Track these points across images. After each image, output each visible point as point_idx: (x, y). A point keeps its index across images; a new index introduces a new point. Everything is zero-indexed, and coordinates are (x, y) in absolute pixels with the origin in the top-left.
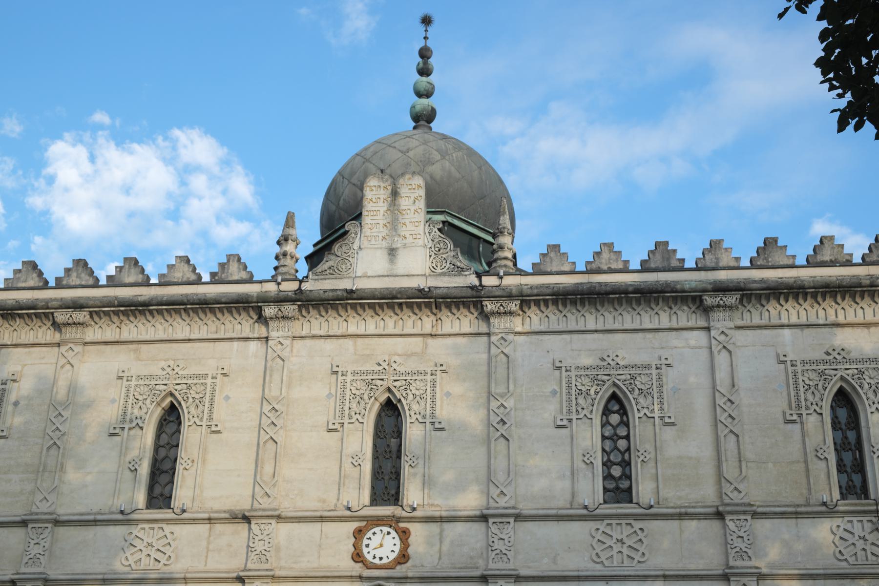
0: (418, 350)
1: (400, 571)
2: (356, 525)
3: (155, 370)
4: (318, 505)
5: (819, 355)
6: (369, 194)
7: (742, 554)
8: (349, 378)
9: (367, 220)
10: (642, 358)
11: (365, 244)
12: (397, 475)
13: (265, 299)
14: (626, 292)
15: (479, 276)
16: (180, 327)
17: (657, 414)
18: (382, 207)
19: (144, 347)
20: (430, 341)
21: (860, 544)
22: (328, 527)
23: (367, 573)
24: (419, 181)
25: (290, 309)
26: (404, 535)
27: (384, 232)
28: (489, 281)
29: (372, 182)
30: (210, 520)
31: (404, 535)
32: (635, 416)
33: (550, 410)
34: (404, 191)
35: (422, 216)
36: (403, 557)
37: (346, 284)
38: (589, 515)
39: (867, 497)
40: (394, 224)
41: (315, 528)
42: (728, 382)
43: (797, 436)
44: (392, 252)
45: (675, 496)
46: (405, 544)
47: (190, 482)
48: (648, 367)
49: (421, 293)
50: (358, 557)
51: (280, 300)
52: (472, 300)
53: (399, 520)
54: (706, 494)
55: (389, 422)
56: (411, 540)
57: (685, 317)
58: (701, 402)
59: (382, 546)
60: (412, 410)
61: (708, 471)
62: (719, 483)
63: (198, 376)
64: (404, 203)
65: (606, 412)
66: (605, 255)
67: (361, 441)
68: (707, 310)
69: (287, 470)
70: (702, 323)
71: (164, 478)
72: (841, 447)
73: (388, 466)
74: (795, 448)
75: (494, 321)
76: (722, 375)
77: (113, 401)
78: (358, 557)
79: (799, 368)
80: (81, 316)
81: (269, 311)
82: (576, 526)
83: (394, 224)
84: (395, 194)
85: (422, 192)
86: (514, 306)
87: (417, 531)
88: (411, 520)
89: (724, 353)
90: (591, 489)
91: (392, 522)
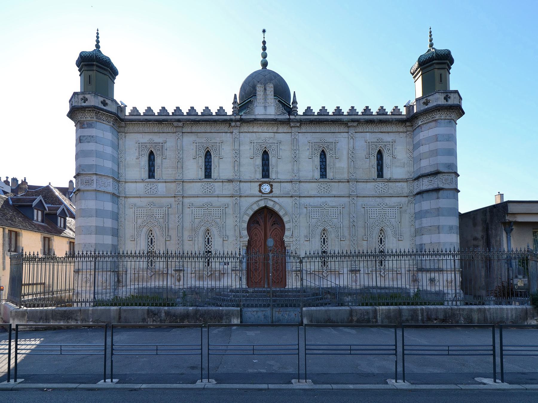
2: (259, 183)
3: (203, 140)
4: (249, 178)
5: (375, 140)
6: (258, 89)
7: (353, 191)
8: (255, 144)
9: (258, 97)
10: (331, 140)
11: (258, 105)
12: (268, 170)
13: (231, 120)
16: (208, 128)
17: (334, 156)
18: (262, 93)
19: (199, 134)
20: (276, 134)
21: (381, 189)
23: (263, 195)
24: (272, 86)
25: (238, 123)
27: (263, 101)
28: (292, 117)
29: (259, 85)
31: (271, 186)
32: (328, 156)
34: (268, 88)
35: (273, 97)
36: (271, 191)
37: (253, 117)
38: (316, 181)
39: (382, 177)
40: (265, 99)
41: (249, 184)
42: (352, 147)
43: (368, 162)
44: (265, 107)
45: (338, 177)
46: (272, 188)
47: (216, 171)
48: (332, 143)
49: (275, 120)
50: (260, 191)
51: (236, 121)
52: (287, 122)
53: (270, 182)
54: (345, 176)
55: (265, 156)
57: (342, 129)
58: (345, 153)
59: (266, 188)
61: (346, 170)
62: (348, 173)
63: (215, 143)
64: (268, 92)
65: (321, 155)
66: (323, 110)
67: (259, 161)
68: (349, 127)
69: (242, 169)
70: (347, 131)
71: (208, 171)
72: (378, 165)
73: (265, 168)
75: (293, 129)
76: (351, 145)
77: (193, 149)
78: (260, 191)
79: (370, 144)
81: (233, 124)
82: (314, 184)
83: (265, 99)
84: (265, 89)
85: (273, 89)
87: (275, 185)
88: (273, 182)
89: (352, 139)
90: (317, 174)
91: (268, 183)
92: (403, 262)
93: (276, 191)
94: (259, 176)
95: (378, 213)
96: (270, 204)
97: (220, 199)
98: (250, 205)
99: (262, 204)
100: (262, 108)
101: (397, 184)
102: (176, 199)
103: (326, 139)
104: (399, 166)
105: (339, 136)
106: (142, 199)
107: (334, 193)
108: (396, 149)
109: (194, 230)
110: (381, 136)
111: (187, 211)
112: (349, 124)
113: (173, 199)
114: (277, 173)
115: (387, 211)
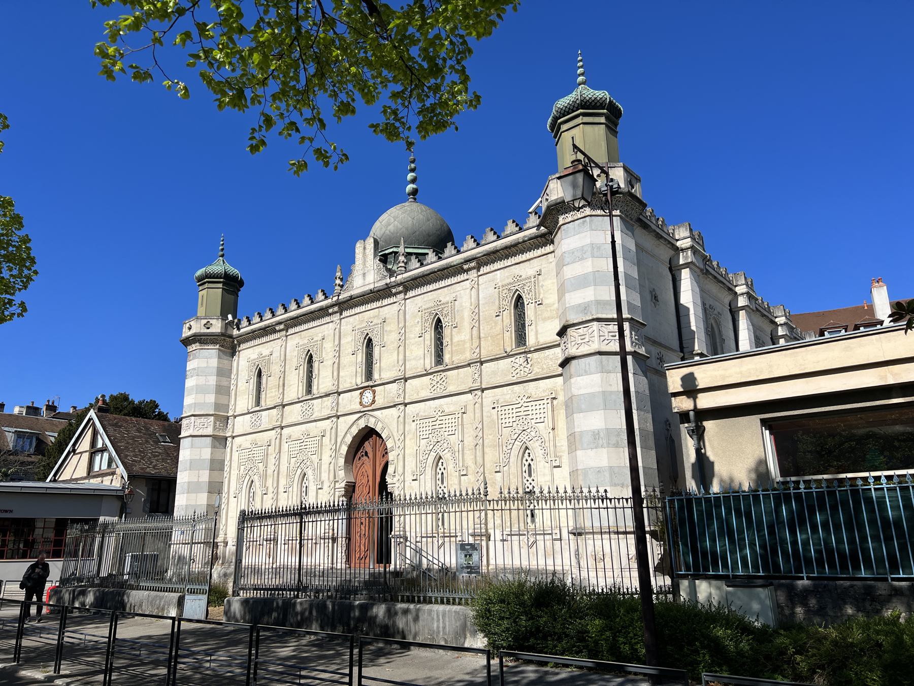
1: (373, 407)
9: (357, 263)
25: (336, 309)
26: (374, 392)
30: (321, 397)
33: (418, 330)
36: (374, 402)
43: (500, 322)
53: (372, 387)
54: (467, 356)
58: (467, 314)
60: (375, 342)
64: (367, 251)
67: (361, 357)
74: (499, 327)
81: (330, 311)
84: (365, 248)
86: (401, 288)
92: (563, 512)
93: (380, 402)
94: (360, 380)
95: (514, 415)
98: (348, 429)
99: (362, 424)
101: (547, 352)
103: (441, 299)
104: (549, 318)
105: (459, 289)
107: (452, 389)
108: (542, 286)
110: (516, 270)
111: (285, 447)
115: (530, 408)
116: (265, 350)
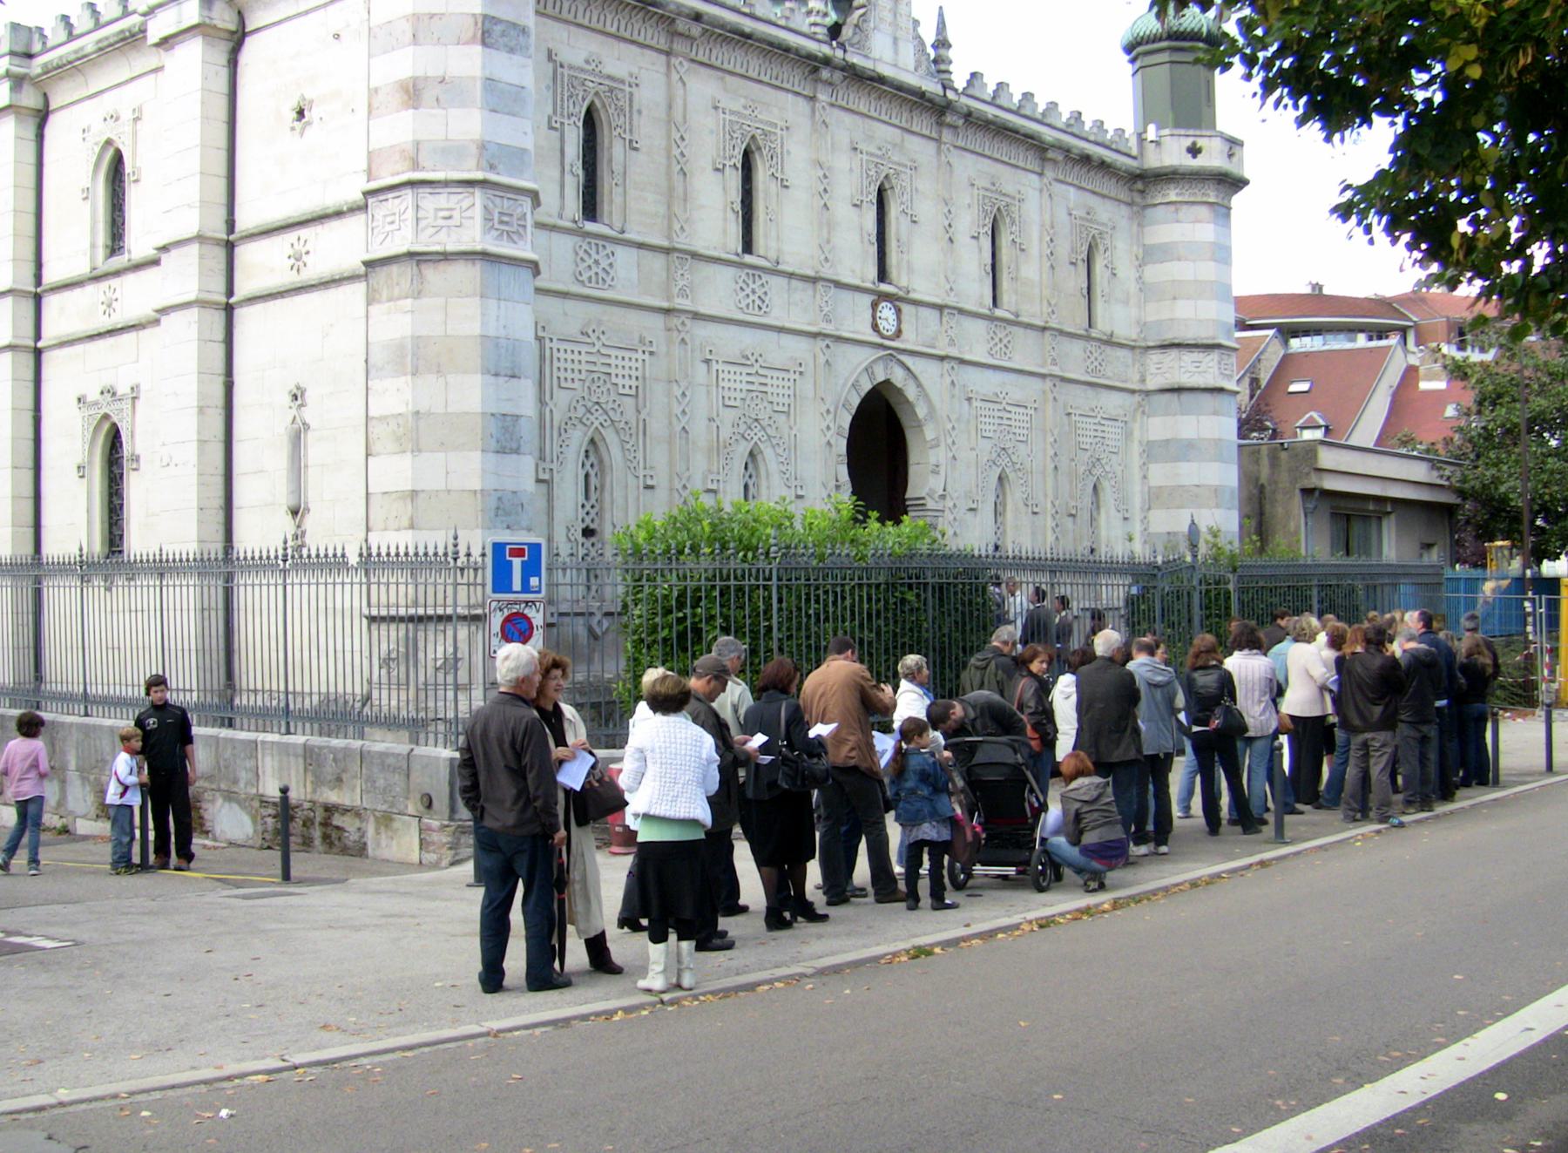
0: (898, 141)
14: (1017, 132)
15: (944, 88)
16: (755, 65)
19: (728, 78)
22: (858, 295)
25: (838, 75)
30: (791, 275)
36: (899, 333)
37: (868, 64)
50: (875, 327)
56: (904, 317)
58: (1035, 233)
70: (1038, 169)
78: (875, 327)
80: (696, 30)
81: (825, 74)
96: (898, 377)
97: (786, 339)
100: (889, 41)
102: (675, 321)
106: (570, 304)
109: (719, 449)
110: (1093, 201)
112: (1050, 154)
113: (658, 321)
114: (910, 270)
116: (619, 61)
